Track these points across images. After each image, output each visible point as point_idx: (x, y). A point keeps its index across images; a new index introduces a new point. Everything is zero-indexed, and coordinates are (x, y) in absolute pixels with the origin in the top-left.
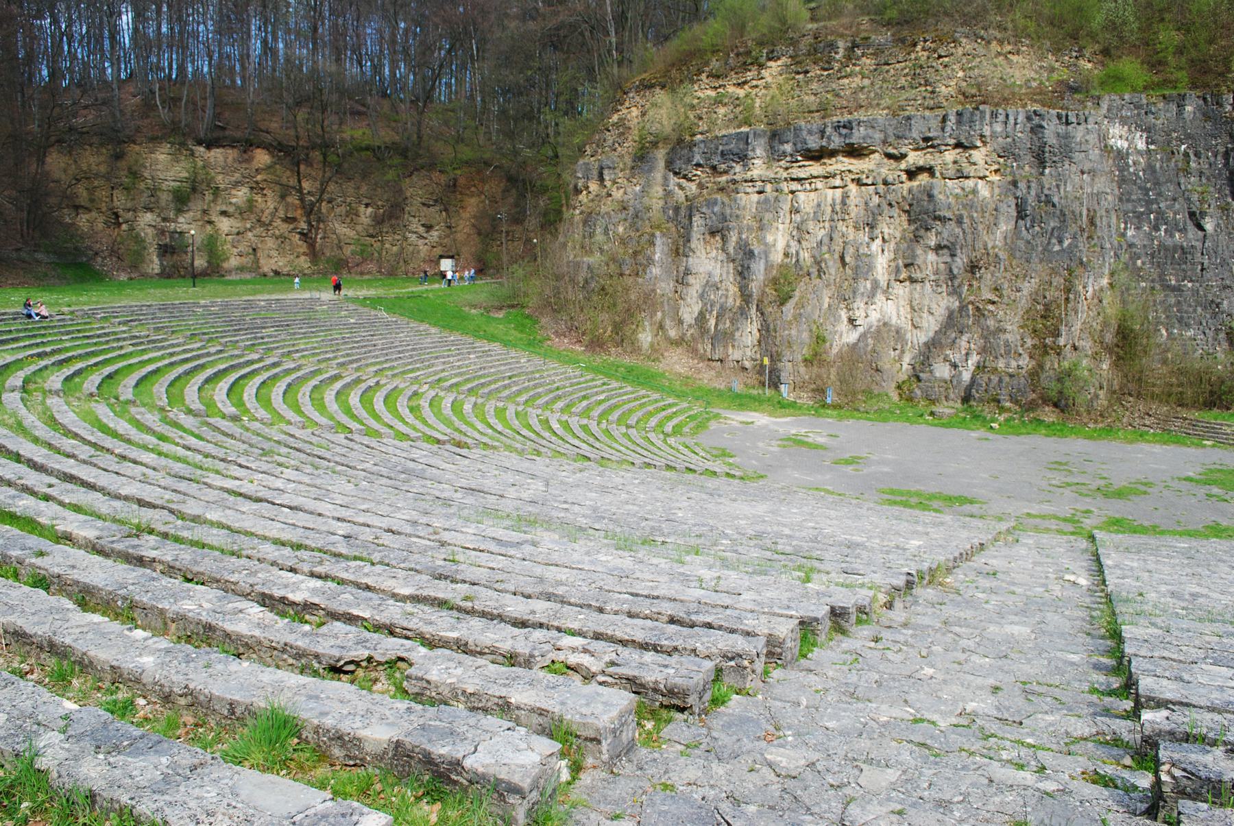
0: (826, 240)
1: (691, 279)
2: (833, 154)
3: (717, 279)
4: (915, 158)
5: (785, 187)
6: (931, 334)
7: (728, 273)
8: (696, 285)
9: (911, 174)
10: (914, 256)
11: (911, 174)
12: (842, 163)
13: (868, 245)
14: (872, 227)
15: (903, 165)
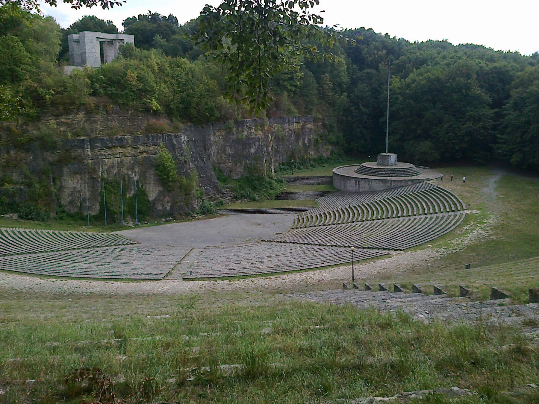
0: (117, 174)
1: (65, 190)
2: (115, 147)
3: (79, 189)
4: (142, 148)
5: (100, 157)
6: (154, 198)
7: (85, 187)
8: (67, 192)
9: (141, 153)
10: (146, 177)
11: (141, 153)
12: (119, 150)
13: (132, 174)
14: (133, 169)
15: (139, 151)
